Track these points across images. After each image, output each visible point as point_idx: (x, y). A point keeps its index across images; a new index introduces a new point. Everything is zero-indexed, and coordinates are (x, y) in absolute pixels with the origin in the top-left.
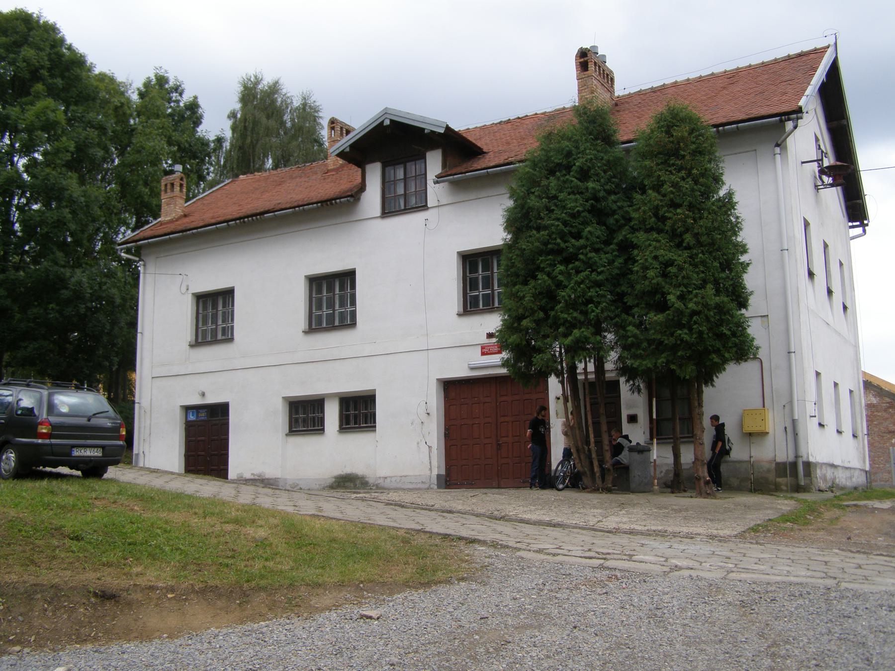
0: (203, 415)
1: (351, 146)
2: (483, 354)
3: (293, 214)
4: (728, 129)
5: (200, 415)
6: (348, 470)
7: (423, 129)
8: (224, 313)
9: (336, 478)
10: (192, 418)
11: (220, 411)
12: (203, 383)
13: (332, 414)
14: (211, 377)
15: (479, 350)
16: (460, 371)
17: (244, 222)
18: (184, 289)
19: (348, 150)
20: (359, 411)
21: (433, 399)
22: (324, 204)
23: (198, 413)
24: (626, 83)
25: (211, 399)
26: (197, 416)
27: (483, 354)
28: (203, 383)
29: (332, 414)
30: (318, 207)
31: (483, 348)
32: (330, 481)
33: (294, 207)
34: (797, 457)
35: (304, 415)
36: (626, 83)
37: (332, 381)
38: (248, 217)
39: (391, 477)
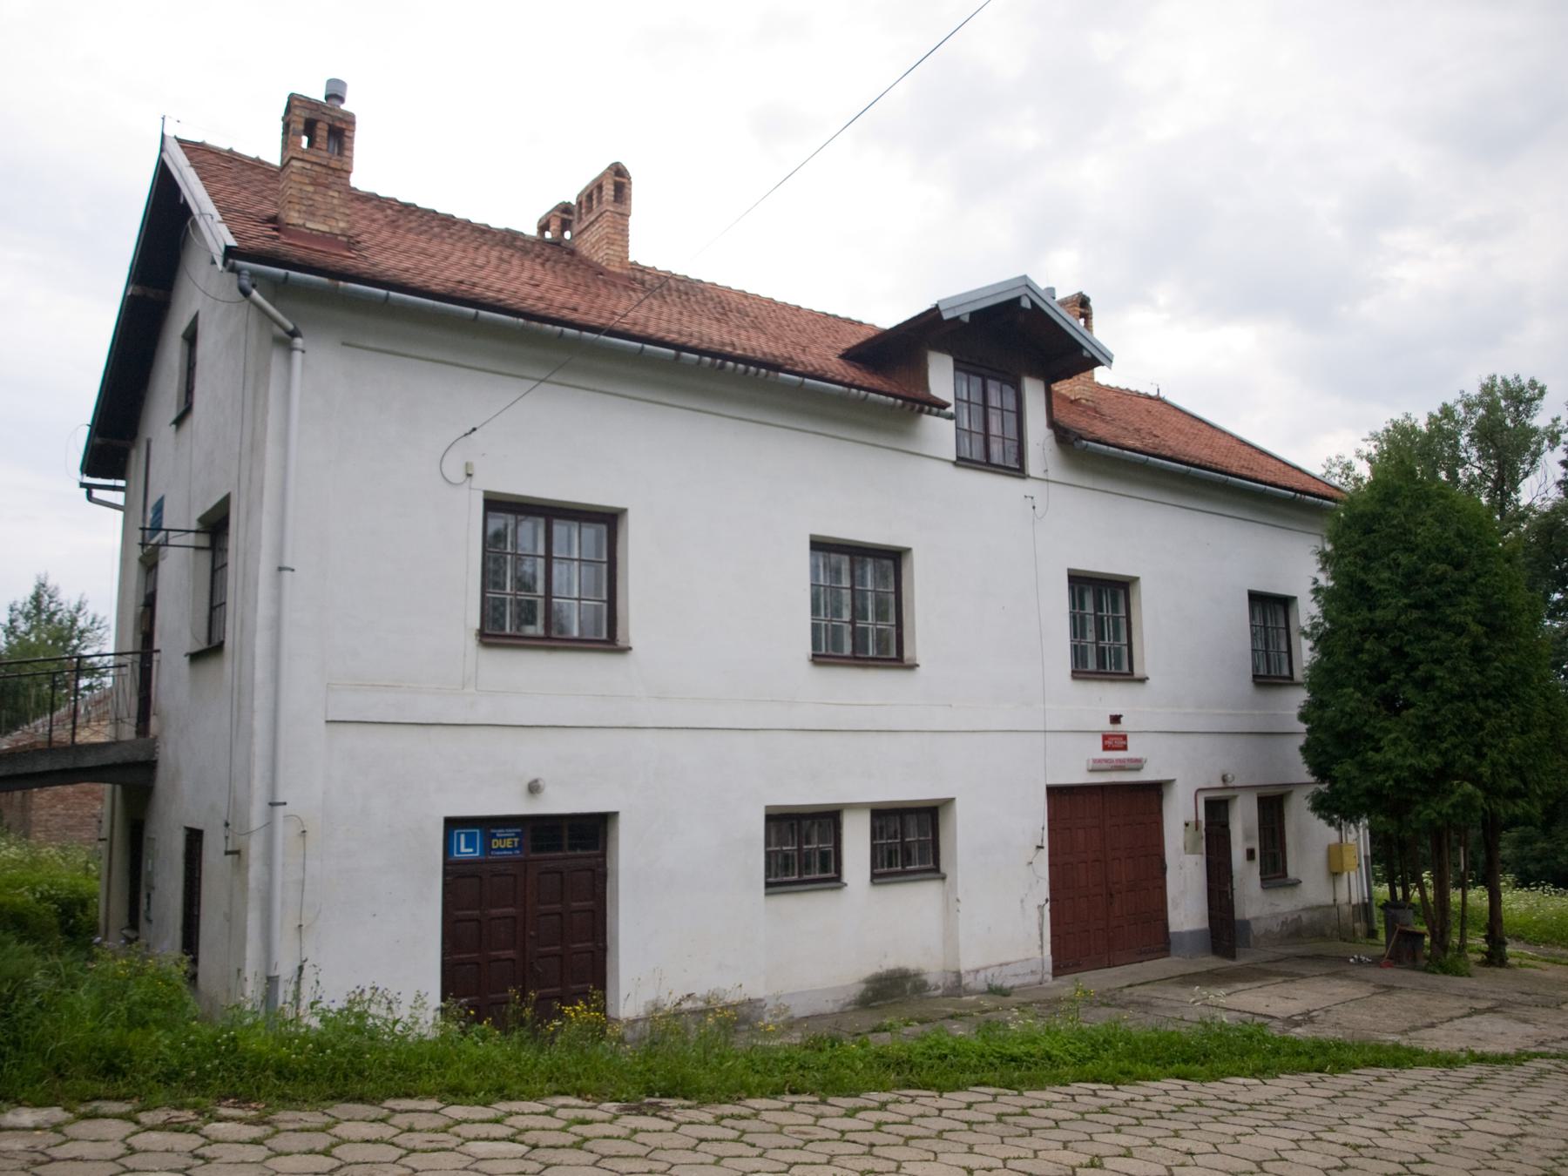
0: (505, 842)
1: (973, 314)
2: (1106, 748)
3: (841, 398)
4: (650, 352)
5: (496, 843)
6: (891, 963)
7: (1081, 347)
8: (837, 612)
9: (867, 981)
10: (464, 851)
11: (586, 837)
12: (533, 757)
13: (856, 842)
14: (537, 739)
15: (1098, 742)
16: (1076, 774)
17: (722, 367)
18: (455, 472)
19: (966, 319)
20: (911, 839)
21: (1035, 818)
22: (909, 405)
23: (488, 839)
24: (372, 171)
25: (558, 802)
26: (487, 848)
27: (1106, 748)
28: (533, 757)
29: (856, 842)
30: (893, 407)
31: (1105, 738)
32: (856, 991)
33: (850, 386)
34: (1370, 898)
35: (800, 848)
36: (372, 171)
37: (859, 778)
38: (737, 359)
39: (985, 968)
